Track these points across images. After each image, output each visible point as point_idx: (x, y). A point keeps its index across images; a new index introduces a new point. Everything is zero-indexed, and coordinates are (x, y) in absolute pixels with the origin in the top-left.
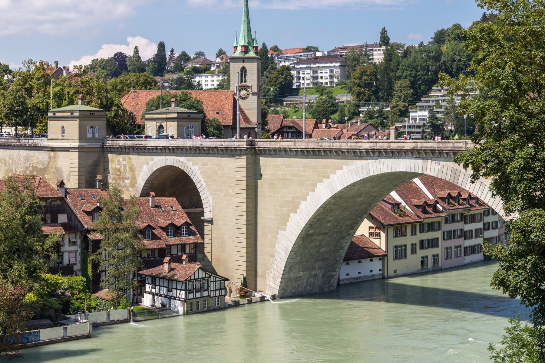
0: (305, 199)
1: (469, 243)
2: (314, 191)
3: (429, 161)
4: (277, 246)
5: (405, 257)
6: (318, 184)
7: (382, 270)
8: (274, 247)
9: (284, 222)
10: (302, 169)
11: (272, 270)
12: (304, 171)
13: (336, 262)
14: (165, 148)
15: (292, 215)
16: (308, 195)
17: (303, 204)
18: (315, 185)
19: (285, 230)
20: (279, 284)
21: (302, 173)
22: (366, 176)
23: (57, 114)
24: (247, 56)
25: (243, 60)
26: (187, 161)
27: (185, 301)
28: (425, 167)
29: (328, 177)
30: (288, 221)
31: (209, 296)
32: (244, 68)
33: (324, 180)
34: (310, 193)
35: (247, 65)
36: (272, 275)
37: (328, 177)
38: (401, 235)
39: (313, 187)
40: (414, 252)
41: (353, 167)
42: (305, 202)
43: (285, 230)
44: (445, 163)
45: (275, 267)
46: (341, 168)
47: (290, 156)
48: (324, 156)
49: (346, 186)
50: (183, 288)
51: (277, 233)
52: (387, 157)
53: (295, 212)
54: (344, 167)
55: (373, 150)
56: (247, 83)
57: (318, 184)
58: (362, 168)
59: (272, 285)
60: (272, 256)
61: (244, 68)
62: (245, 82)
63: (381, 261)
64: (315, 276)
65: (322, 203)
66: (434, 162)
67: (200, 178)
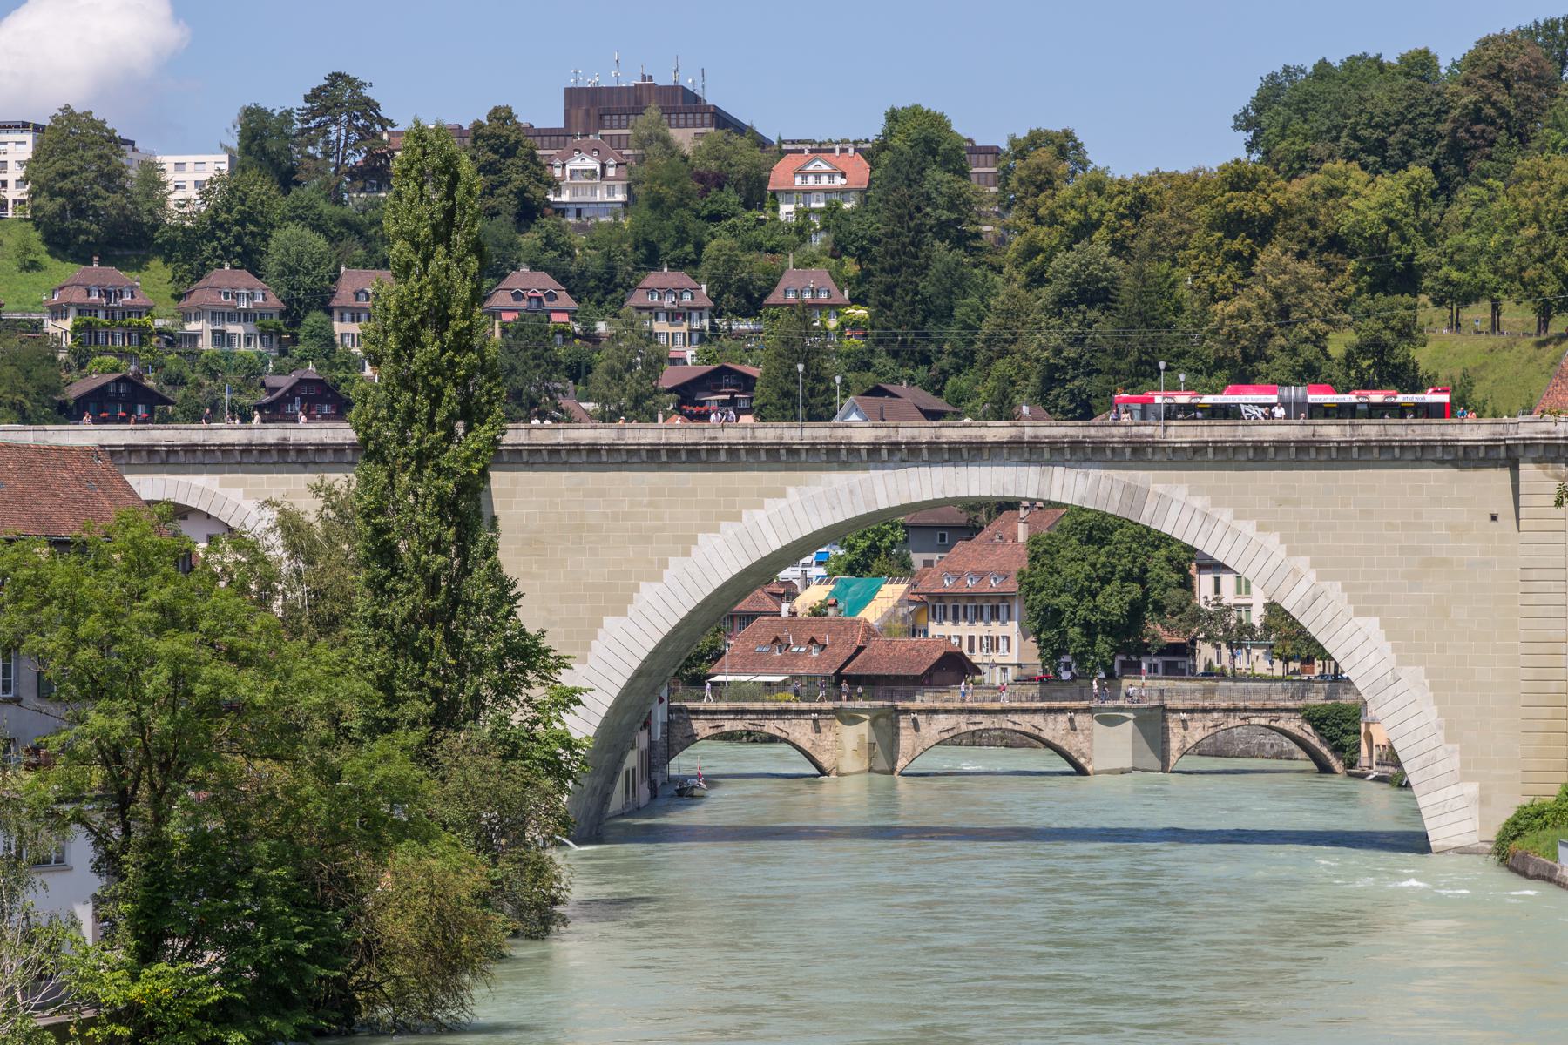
0: (657, 577)
2: (687, 553)
3: (1059, 470)
6: (701, 537)
10: (645, 500)
12: (650, 504)
17: (648, 593)
21: (645, 509)
22: (863, 511)
26: (222, 485)
28: (1048, 483)
29: (738, 518)
30: (595, 638)
33: (724, 525)
37: (738, 518)
39: (685, 545)
41: (821, 489)
42: (657, 586)
44: (1103, 472)
46: (781, 494)
47: (601, 466)
48: (724, 462)
52: (930, 463)
53: (624, 613)
54: (791, 490)
57: (701, 537)
58: (851, 492)
66: (1071, 473)
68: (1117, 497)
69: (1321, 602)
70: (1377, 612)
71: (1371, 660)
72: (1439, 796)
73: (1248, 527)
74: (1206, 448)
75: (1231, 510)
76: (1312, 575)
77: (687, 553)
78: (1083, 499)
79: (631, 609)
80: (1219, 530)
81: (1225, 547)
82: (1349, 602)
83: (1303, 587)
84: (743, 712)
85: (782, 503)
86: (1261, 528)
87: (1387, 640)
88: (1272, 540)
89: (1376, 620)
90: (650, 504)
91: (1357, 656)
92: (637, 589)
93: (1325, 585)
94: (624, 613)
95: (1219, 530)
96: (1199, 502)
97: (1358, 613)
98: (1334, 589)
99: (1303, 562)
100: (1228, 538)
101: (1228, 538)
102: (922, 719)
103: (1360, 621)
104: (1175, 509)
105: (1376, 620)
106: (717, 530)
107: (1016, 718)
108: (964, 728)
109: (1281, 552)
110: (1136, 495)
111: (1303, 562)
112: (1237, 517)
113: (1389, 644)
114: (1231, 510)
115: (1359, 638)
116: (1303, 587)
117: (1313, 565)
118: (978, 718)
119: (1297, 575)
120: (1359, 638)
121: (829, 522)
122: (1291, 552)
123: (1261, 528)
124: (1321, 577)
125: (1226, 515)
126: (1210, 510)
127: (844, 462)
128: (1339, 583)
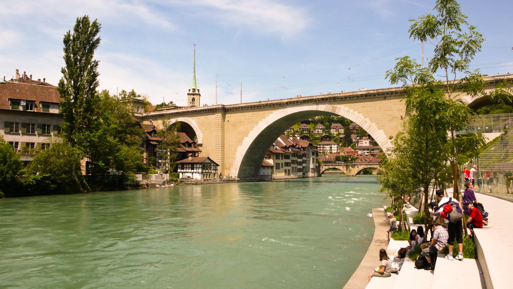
0: (252, 130)
1: (299, 167)
2: (257, 125)
4: (237, 154)
5: (280, 169)
8: (235, 154)
9: (240, 142)
10: (251, 116)
11: (234, 165)
12: (252, 117)
14: (177, 113)
15: (245, 138)
18: (258, 123)
20: (238, 171)
24: (195, 93)
25: (194, 95)
27: (202, 173)
29: (265, 118)
30: (243, 141)
31: (211, 172)
32: (194, 98)
33: (263, 119)
34: (255, 126)
35: (195, 97)
36: (234, 167)
37: (265, 118)
38: (278, 159)
39: (257, 123)
40: (282, 167)
42: (253, 131)
45: (236, 163)
46: (272, 113)
49: (275, 120)
50: (201, 167)
51: (237, 147)
53: (247, 136)
56: (195, 105)
57: (260, 122)
59: (234, 172)
60: (234, 158)
61: (194, 98)
62: (194, 104)
63: (271, 169)
64: (252, 169)
65: (262, 130)
67: (196, 125)
68: (331, 109)
69: (371, 127)
70: (383, 129)
71: (382, 139)
73: (356, 113)
74: (347, 97)
75: (353, 110)
76: (369, 122)
78: (324, 110)
79: (249, 136)
80: (350, 114)
82: (377, 127)
83: (367, 124)
84: (333, 165)
85: (272, 115)
86: (359, 113)
87: (385, 134)
88: (361, 115)
89: (382, 131)
90: (252, 117)
91: (379, 138)
92: (249, 132)
93: (372, 124)
94: (247, 136)
95: (350, 114)
96: (347, 109)
97: (379, 129)
98: (374, 125)
99: (367, 119)
100: (352, 115)
101: (352, 115)
102: (359, 166)
103: (379, 131)
104: (342, 110)
105: (382, 131)
106: (262, 120)
107: (374, 166)
108: (366, 167)
109: (363, 118)
110: (335, 108)
111: (367, 119)
112: (354, 111)
113: (385, 135)
114: (353, 110)
115: (379, 134)
116: (367, 124)
117: (369, 120)
118: (368, 166)
119: (366, 122)
120: (379, 134)
121: (280, 117)
122: (365, 117)
123: (359, 113)
124: (371, 122)
125: (352, 111)
126: (349, 110)
127: (282, 106)
128: (375, 123)
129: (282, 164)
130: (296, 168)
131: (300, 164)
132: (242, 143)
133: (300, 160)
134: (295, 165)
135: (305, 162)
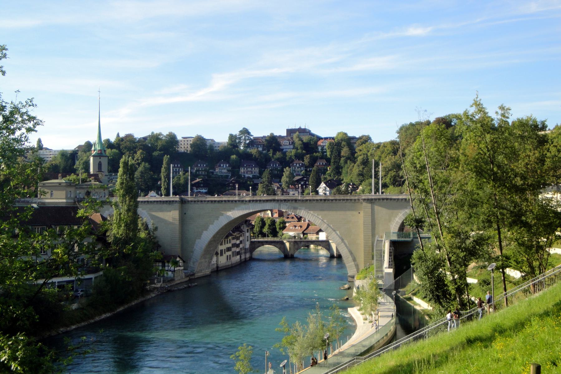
0: (213, 224)
1: (238, 250)
2: (218, 220)
4: (195, 247)
7: (217, 261)
13: (213, 255)
16: (214, 222)
17: (211, 227)
18: (219, 217)
19: (200, 239)
23: (46, 185)
36: (191, 261)
40: (225, 253)
43: (200, 239)
55: (253, 201)
57: (220, 217)
59: (192, 265)
60: (192, 252)
72: (350, 264)
77: (218, 220)
79: (208, 230)
81: (312, 218)
92: (209, 226)
129: (225, 250)
130: (235, 251)
131: (238, 246)
132: (201, 237)
133: (238, 242)
134: (234, 249)
135: (241, 242)
